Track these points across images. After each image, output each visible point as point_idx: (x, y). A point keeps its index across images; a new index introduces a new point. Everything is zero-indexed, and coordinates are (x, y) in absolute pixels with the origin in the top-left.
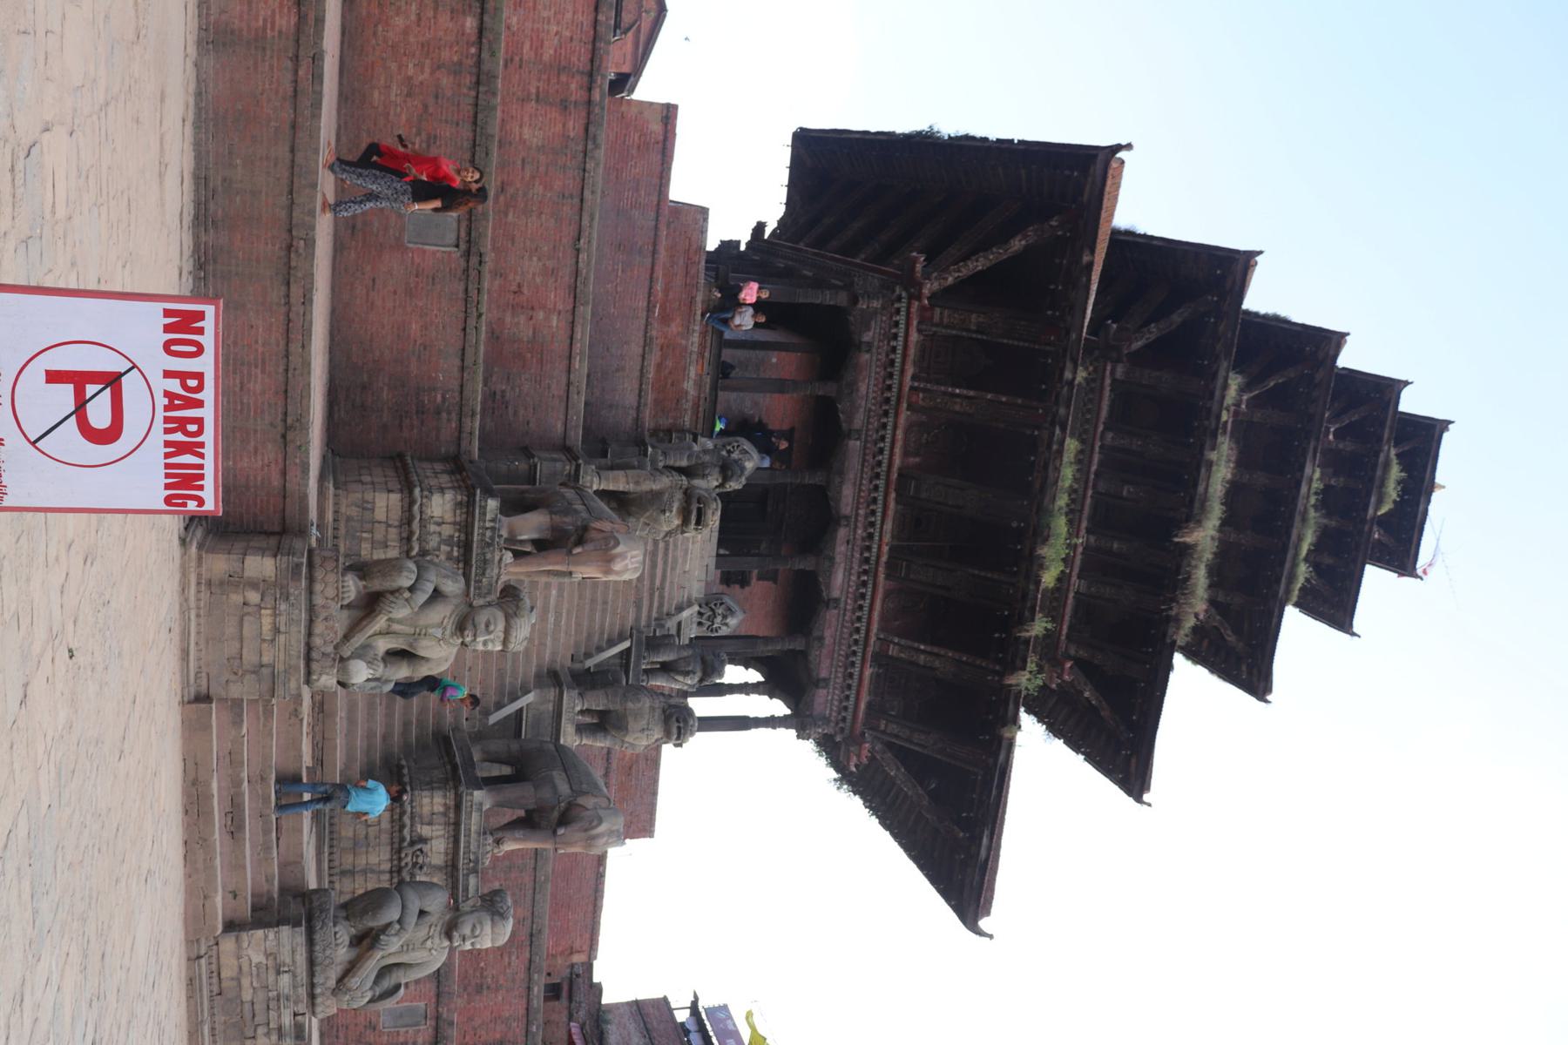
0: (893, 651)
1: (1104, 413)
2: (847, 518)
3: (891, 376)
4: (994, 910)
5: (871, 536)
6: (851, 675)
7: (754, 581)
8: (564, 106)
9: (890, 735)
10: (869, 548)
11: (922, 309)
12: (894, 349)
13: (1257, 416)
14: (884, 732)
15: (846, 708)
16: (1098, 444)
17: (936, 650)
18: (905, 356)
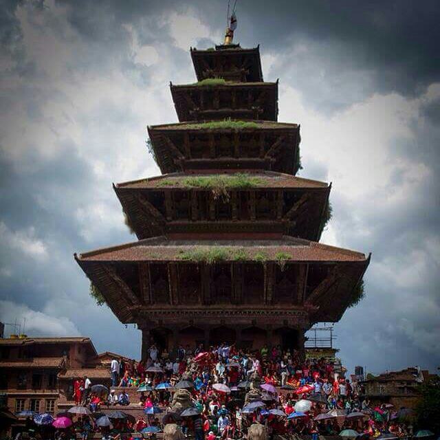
0: (269, 299)
1: (186, 222)
2: (221, 321)
3: (169, 313)
4: (362, 252)
5: (227, 312)
6: (281, 313)
10: (231, 313)
14: (302, 298)
16: (198, 222)
18: (161, 309)
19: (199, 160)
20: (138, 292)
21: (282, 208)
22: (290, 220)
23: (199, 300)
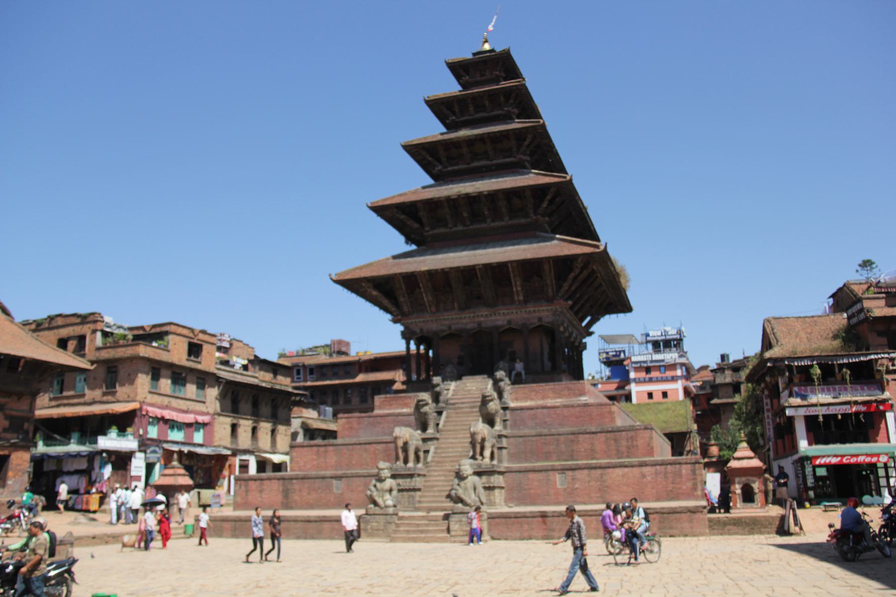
0: (521, 298)
1: (442, 230)
8: (326, 452)
13: (444, 159)
16: (455, 229)
19: (455, 168)
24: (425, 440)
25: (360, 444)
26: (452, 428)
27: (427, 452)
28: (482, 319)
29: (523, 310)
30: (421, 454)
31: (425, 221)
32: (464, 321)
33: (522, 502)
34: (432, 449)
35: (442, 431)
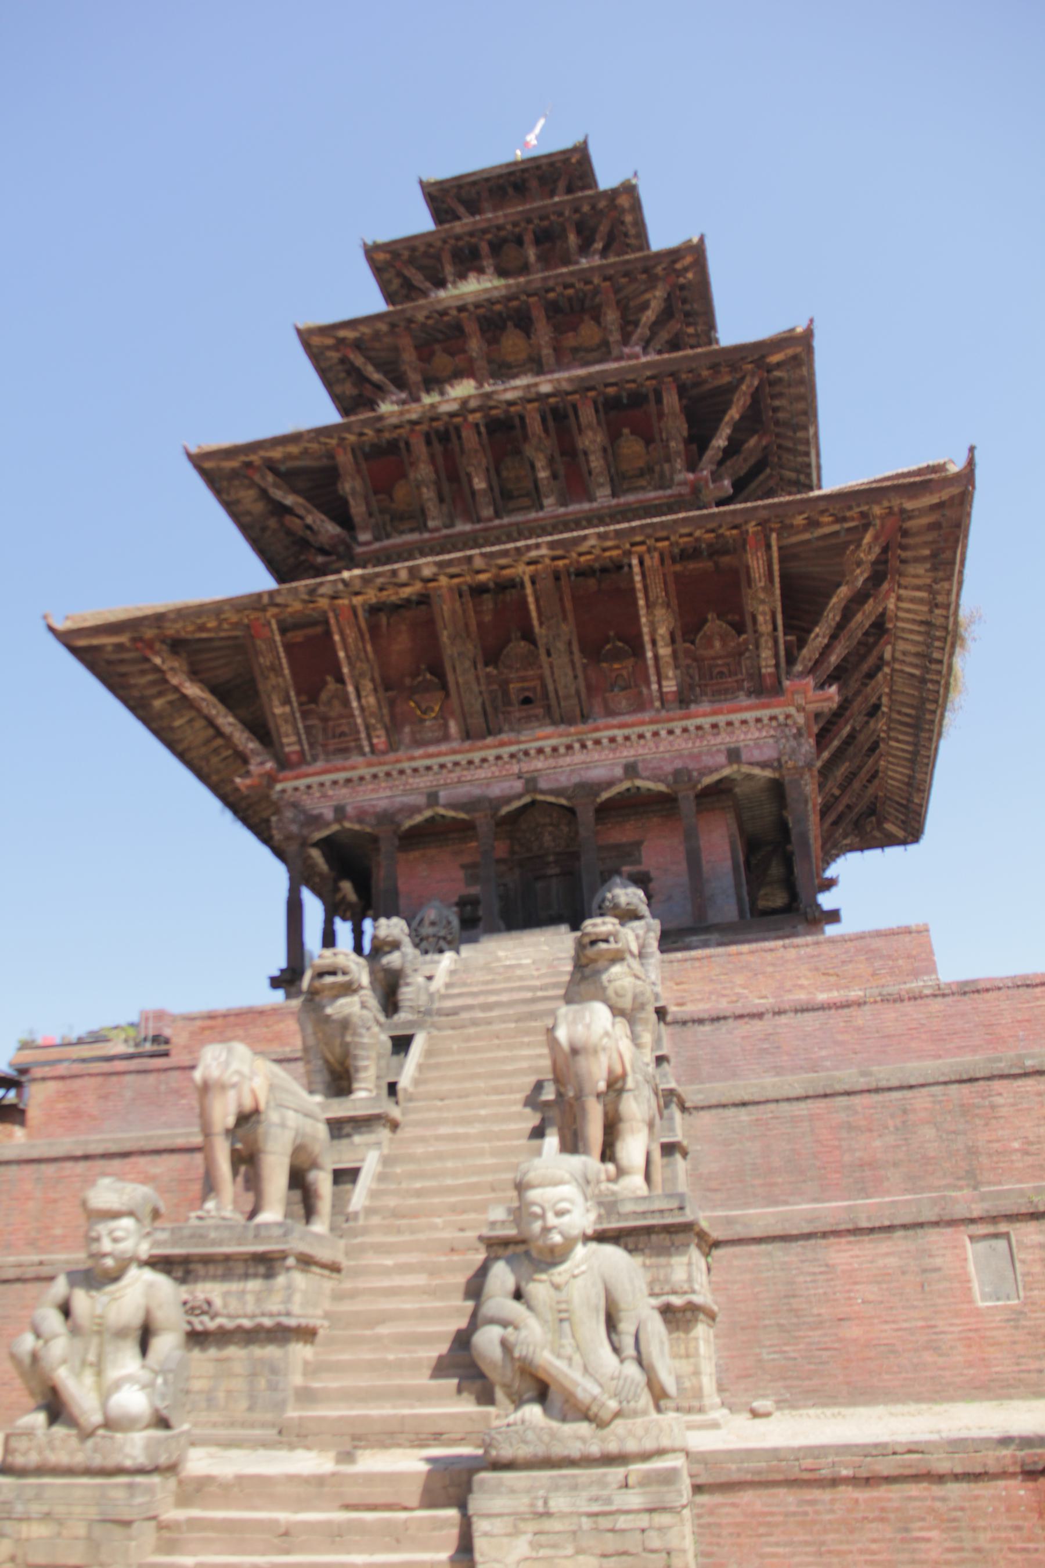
0: (670, 686)
3: (362, 778)
5: (540, 751)
6: (715, 726)
7: (642, 868)
9: (776, 656)
10: (555, 749)
11: (284, 763)
12: (335, 783)
14: (777, 666)
15: (758, 720)
16: (445, 532)
17: (647, 638)
18: (337, 770)
20: (261, 730)
21: (681, 447)
22: (716, 477)
23: (453, 727)
24: (338, 1128)
25: (87, 1157)
26: (446, 1087)
27: (345, 1176)
28: (539, 764)
29: (677, 726)
30: (323, 1181)
31: (357, 509)
32: (481, 774)
33: (810, 1383)
34: (370, 1165)
35: (410, 1098)
